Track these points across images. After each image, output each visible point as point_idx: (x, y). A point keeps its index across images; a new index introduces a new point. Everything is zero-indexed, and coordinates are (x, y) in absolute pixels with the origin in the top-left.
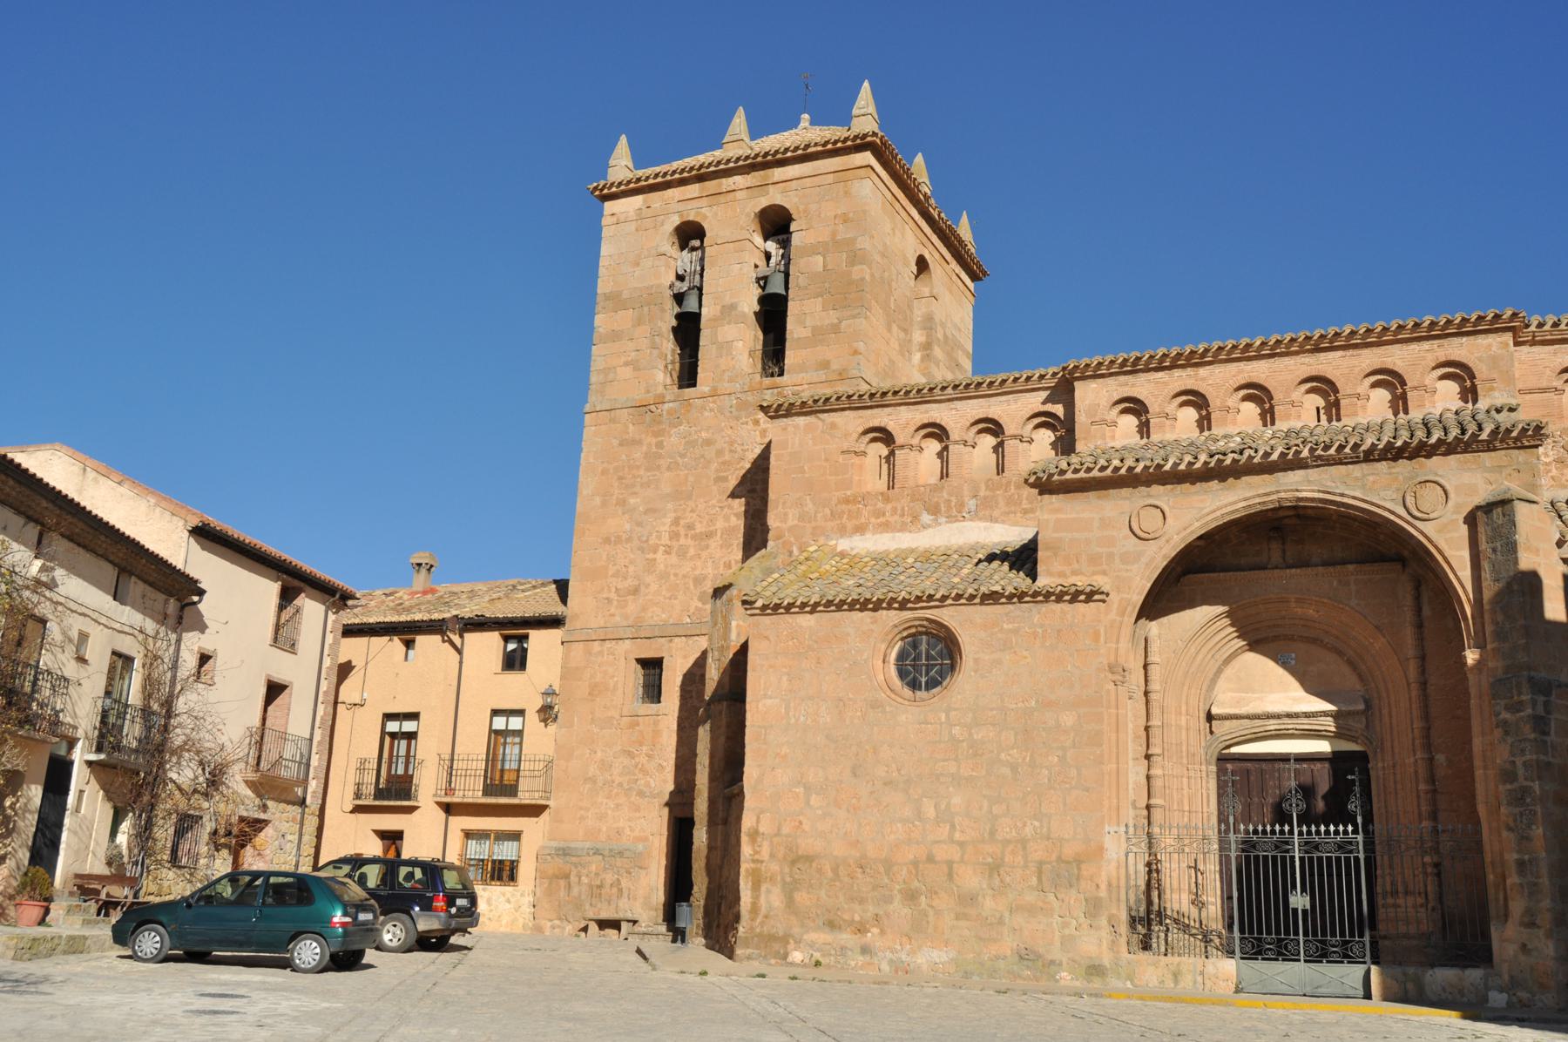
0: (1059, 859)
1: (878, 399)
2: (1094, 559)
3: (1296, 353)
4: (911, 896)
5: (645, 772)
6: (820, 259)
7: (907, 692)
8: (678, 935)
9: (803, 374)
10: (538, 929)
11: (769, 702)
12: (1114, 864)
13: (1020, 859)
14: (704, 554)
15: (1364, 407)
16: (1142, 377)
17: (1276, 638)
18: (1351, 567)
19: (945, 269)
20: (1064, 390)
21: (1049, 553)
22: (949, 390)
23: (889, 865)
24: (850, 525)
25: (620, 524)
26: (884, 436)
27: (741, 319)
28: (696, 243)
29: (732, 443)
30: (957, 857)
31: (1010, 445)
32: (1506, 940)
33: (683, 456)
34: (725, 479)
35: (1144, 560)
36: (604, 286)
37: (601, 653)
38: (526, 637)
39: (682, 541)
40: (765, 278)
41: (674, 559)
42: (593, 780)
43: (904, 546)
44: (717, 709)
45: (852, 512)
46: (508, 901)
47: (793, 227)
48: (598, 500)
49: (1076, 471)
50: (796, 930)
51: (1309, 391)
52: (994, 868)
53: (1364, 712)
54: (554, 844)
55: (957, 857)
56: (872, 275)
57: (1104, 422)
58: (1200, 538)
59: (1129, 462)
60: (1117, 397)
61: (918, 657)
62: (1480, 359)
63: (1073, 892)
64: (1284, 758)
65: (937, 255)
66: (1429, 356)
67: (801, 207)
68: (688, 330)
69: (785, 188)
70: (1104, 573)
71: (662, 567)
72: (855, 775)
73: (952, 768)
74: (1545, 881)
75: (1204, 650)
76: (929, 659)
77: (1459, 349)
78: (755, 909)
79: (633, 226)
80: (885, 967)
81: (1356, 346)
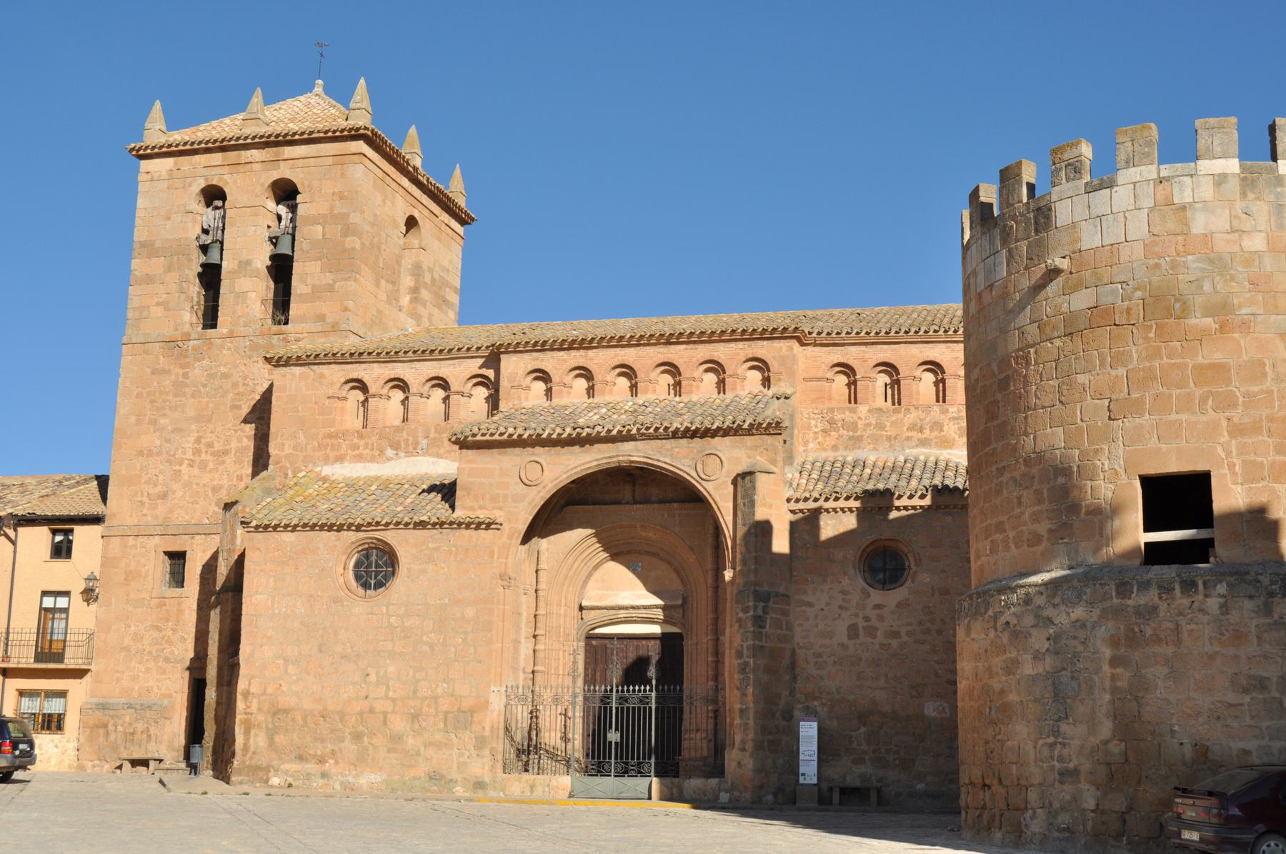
0: (459, 709)
1: (357, 357)
2: (494, 499)
3: (655, 344)
4: (357, 737)
5: (170, 643)
6: (320, 228)
7: (361, 591)
8: (194, 768)
9: (303, 331)
10: (81, 768)
11: (259, 597)
12: (496, 713)
13: (432, 710)
14: (221, 468)
15: (698, 387)
16: (549, 354)
17: (629, 552)
19: (434, 220)
20: (493, 358)
22: (410, 354)
23: (342, 715)
24: (332, 455)
25: (151, 440)
26: (361, 385)
27: (256, 274)
28: (219, 203)
29: (245, 377)
30: (390, 709)
31: (454, 398)
32: (732, 758)
33: (205, 386)
34: (239, 407)
35: (528, 500)
36: (139, 235)
37: (134, 546)
38: (72, 531)
39: (203, 456)
40: (277, 238)
41: (196, 471)
42: (127, 649)
43: (372, 474)
44: (224, 595)
45: (334, 445)
46: (56, 746)
47: (299, 197)
48: (133, 419)
49: (483, 435)
50: (275, 763)
51: (663, 372)
52: (415, 717)
53: (682, 606)
54: (95, 700)
55: (390, 709)
56: (363, 244)
57: (520, 387)
58: (573, 482)
59: (520, 431)
60: (530, 369)
61: (369, 565)
62: (774, 358)
63: (468, 732)
64: (610, 637)
65: (426, 212)
66: (742, 353)
67: (306, 183)
68: (211, 277)
69: (293, 164)
70: (500, 509)
71: (186, 477)
72: (321, 651)
73: (389, 646)
74: (751, 722)
75: (580, 560)
76: (376, 568)
77: (762, 349)
78: (246, 748)
79: (165, 184)
80: (337, 786)
81: (694, 342)
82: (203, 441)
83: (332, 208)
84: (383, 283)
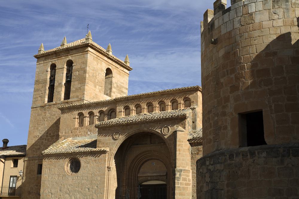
2: (107, 144)
18: (162, 144)
21: (99, 142)
41: (47, 141)
53: (166, 175)
76: (76, 166)
82: (49, 133)
83: (81, 66)
84: (97, 87)
